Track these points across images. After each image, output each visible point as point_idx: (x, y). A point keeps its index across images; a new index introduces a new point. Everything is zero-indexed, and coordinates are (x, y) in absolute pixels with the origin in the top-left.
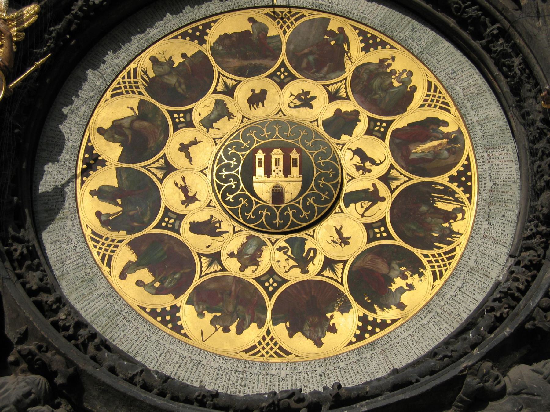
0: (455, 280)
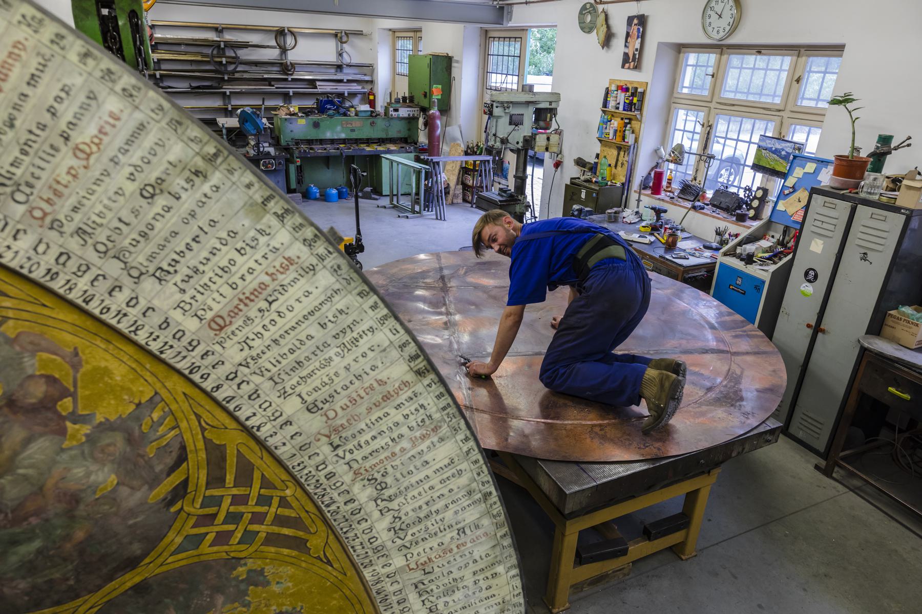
0: (341, 500)
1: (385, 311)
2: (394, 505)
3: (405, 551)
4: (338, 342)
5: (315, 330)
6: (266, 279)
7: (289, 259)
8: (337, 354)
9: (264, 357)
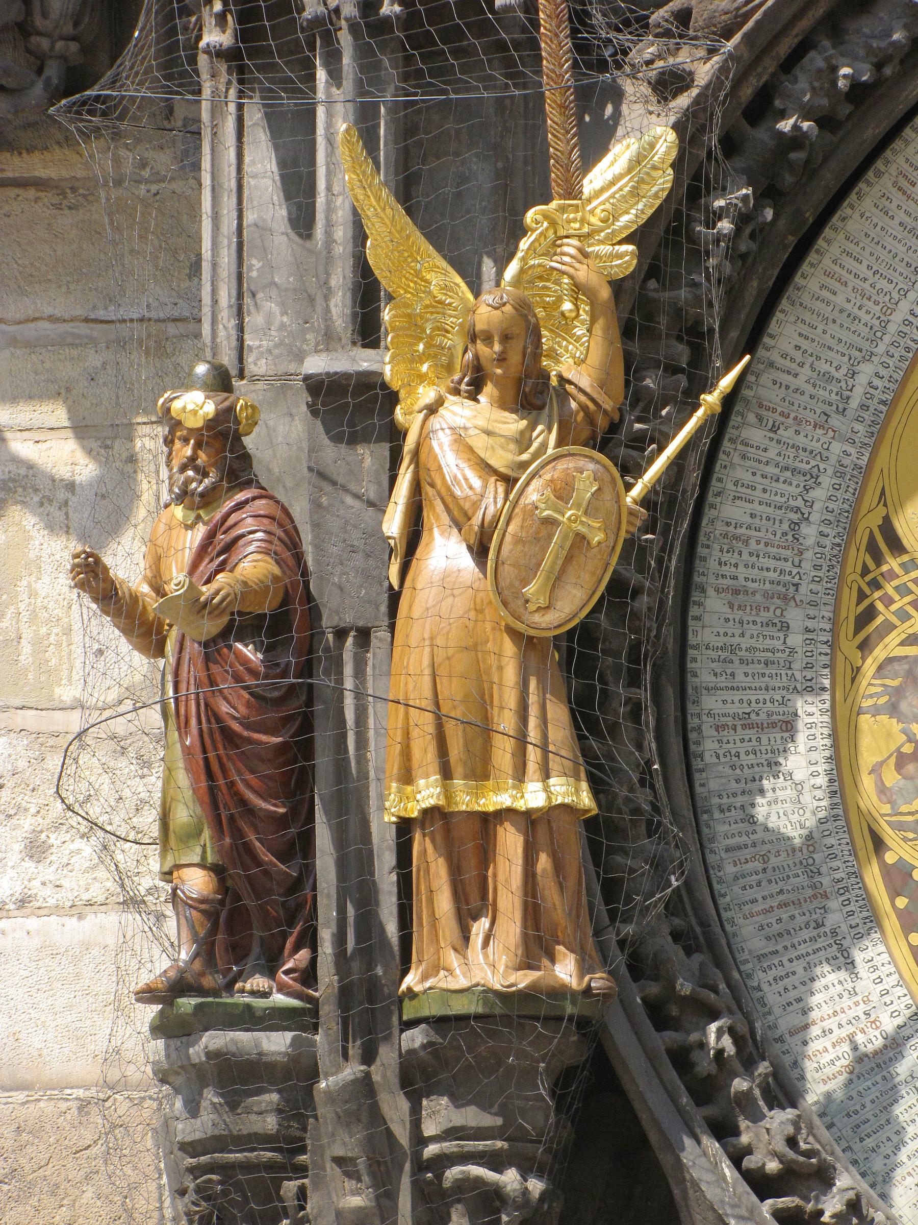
0: (827, 542)
1: (690, 651)
2: (800, 503)
3: (825, 454)
4: (733, 657)
5: (740, 677)
6: (739, 728)
7: (717, 730)
8: (740, 649)
9: (781, 685)
